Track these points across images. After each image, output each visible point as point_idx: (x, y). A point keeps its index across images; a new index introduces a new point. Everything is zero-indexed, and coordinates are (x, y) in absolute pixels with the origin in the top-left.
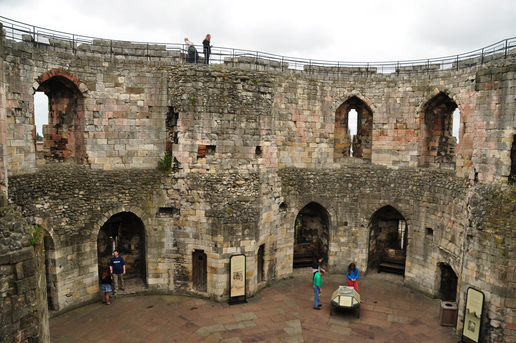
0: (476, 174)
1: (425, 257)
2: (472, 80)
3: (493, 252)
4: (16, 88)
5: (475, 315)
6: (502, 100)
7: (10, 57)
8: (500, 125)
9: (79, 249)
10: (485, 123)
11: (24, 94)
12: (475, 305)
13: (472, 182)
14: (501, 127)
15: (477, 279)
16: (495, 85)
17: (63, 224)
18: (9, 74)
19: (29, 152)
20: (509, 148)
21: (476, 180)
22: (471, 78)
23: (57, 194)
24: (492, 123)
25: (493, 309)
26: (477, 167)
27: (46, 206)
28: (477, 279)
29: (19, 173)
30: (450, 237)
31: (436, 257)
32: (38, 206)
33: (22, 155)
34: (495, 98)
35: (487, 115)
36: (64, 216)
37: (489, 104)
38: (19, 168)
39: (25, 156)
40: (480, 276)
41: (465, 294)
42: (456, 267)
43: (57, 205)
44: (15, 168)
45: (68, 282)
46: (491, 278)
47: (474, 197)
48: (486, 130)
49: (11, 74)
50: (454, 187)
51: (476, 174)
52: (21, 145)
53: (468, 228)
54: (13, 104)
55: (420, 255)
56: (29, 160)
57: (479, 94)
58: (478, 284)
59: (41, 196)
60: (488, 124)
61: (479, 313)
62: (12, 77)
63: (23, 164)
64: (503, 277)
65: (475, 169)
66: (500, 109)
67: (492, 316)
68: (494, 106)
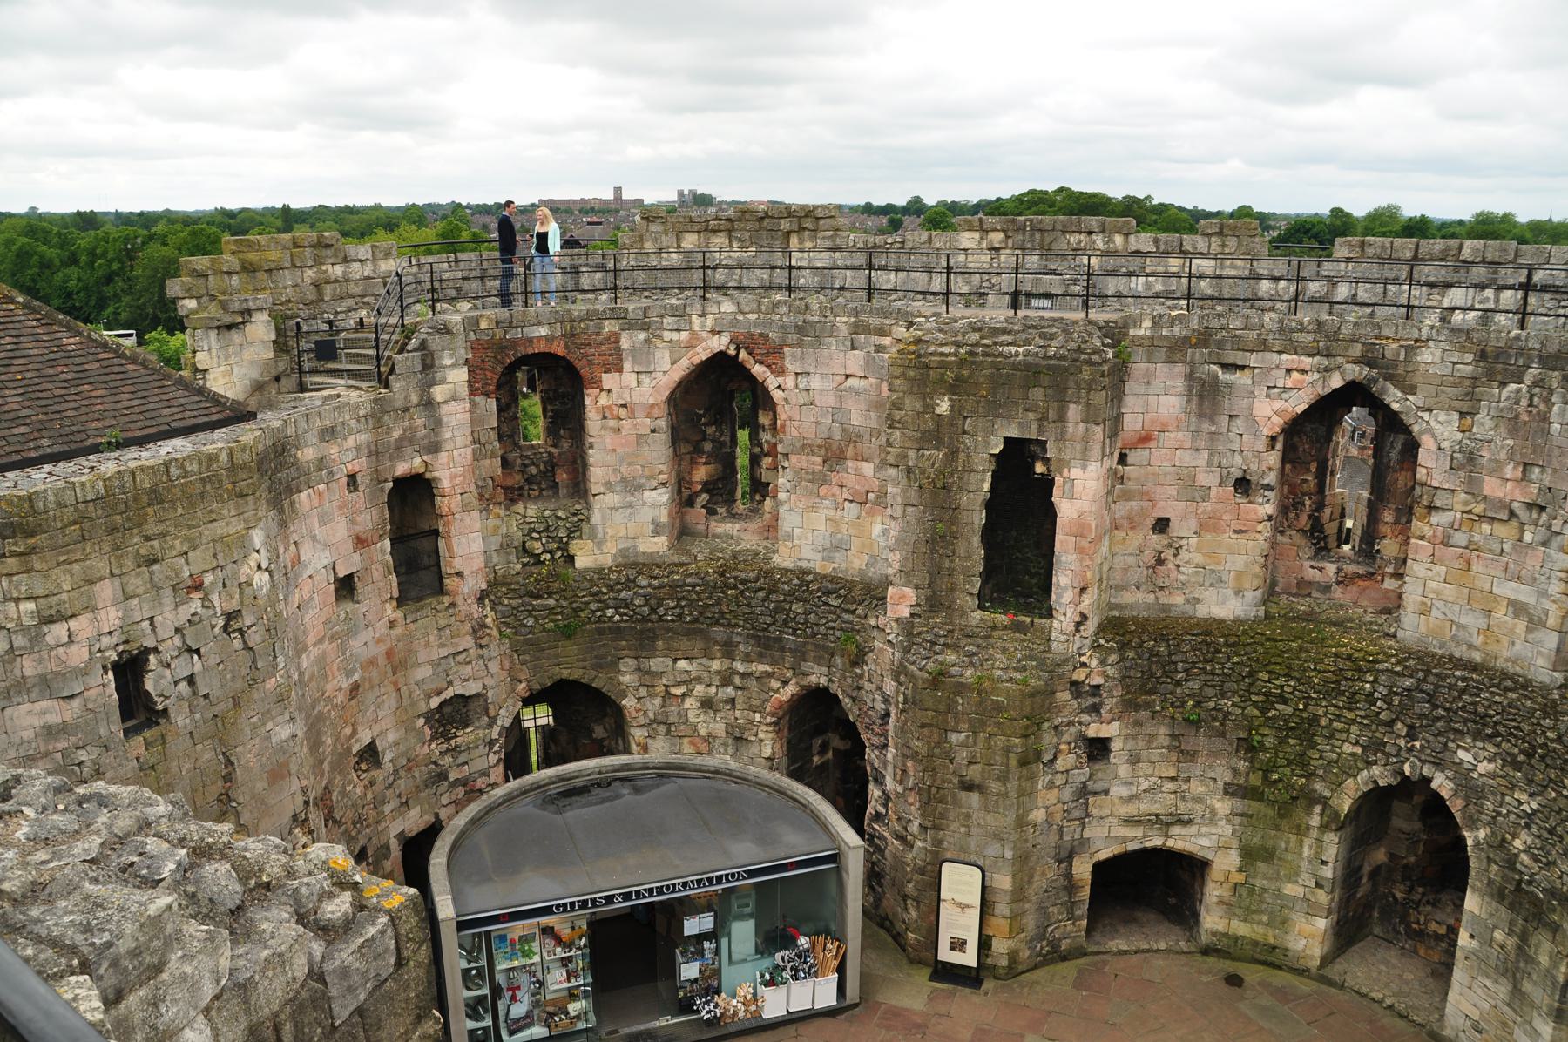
4: (1534, 452)
7: (1533, 372)
9: (1524, 937)
11: (1555, 471)
17: (1517, 843)
18: (1517, 417)
19: (1543, 624)
23: (1521, 758)
27: (1484, 767)
29: (1500, 663)
32: (1462, 754)
33: (1521, 626)
36: (1528, 826)
38: (1506, 654)
39: (1529, 630)
43: (1512, 787)
44: (1493, 648)
45: (1479, 991)
49: (1524, 417)
52: (1523, 598)
54: (1517, 492)
56: (1539, 644)
59: (1477, 736)
62: (1525, 423)
63: (1518, 647)
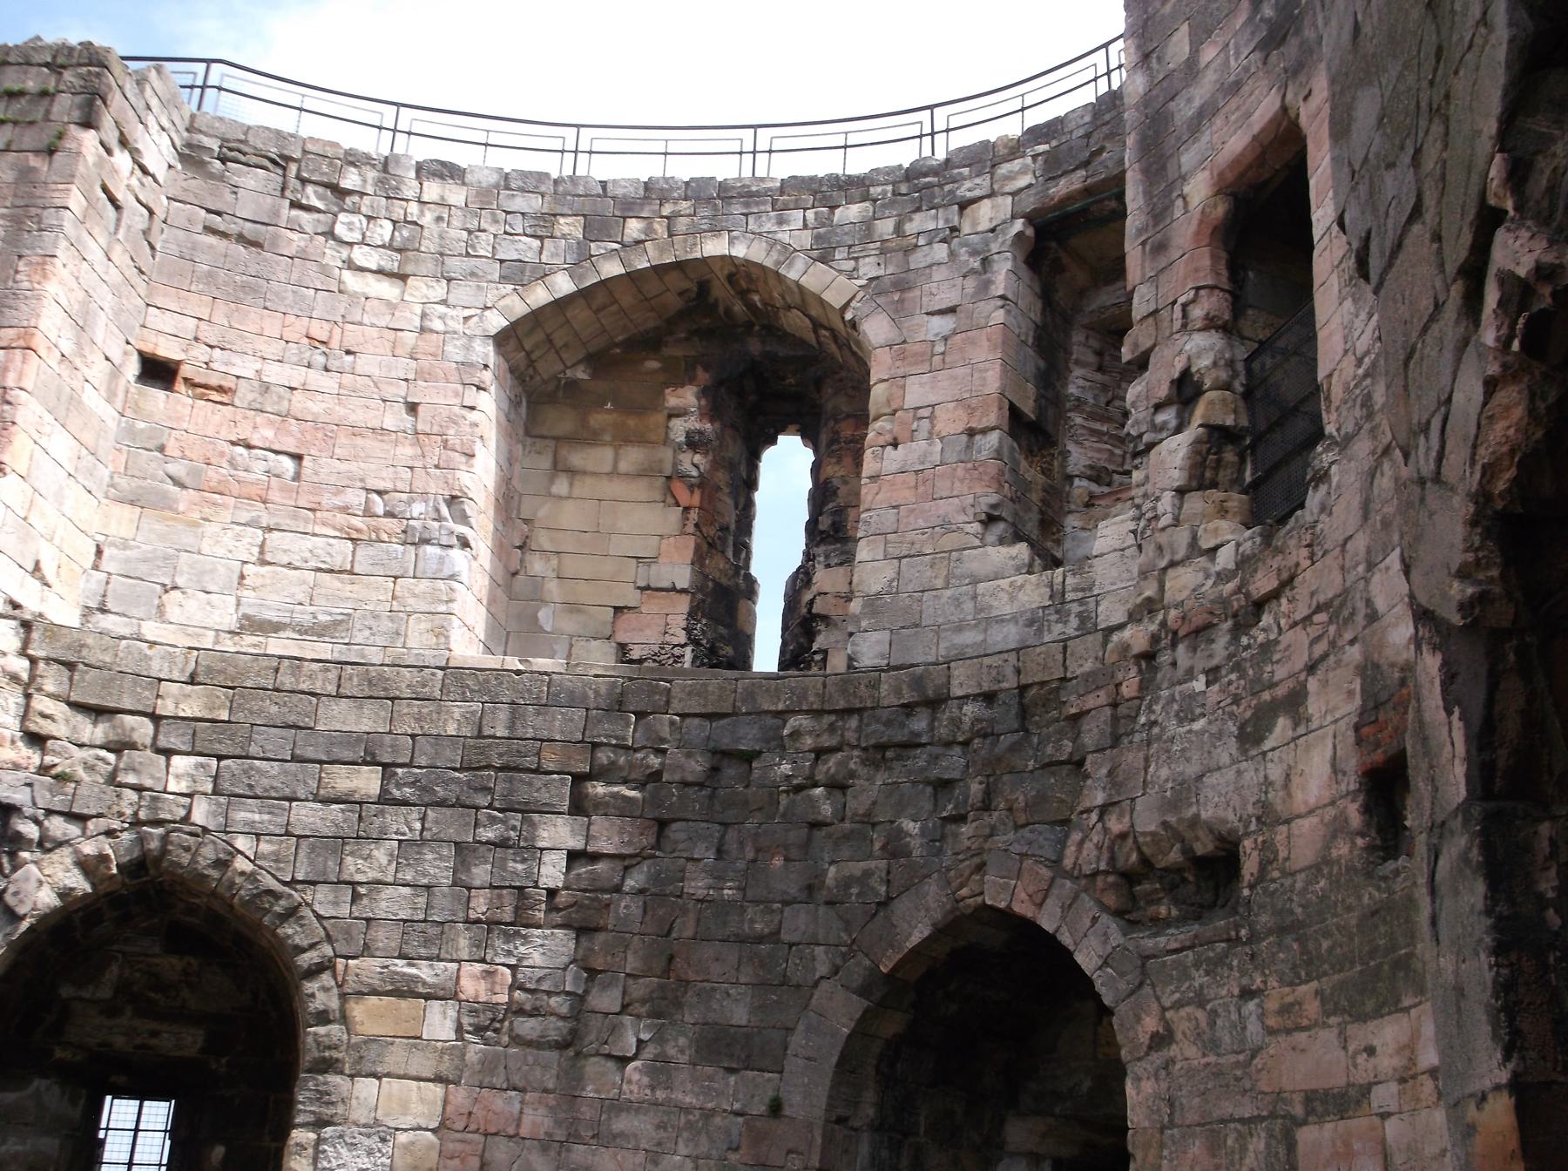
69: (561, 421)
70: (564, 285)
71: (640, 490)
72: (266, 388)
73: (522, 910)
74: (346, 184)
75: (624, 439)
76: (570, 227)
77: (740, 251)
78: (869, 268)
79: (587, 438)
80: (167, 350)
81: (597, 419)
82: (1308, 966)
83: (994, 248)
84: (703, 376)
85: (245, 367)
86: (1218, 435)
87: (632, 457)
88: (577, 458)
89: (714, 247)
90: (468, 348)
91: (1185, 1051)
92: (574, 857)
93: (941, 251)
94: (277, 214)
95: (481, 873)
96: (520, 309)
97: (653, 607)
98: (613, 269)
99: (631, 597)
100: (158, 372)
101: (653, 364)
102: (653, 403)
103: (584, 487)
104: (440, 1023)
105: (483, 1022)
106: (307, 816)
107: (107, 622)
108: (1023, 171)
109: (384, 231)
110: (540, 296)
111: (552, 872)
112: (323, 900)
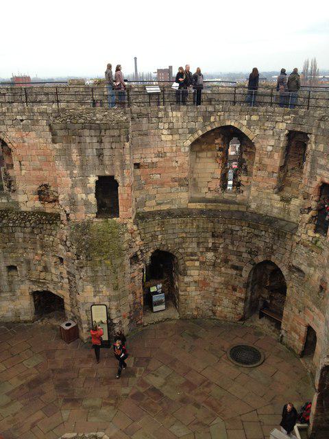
0: (68, 215)
1: (12, 291)
2: (22, 120)
3: (105, 272)
5: (102, 323)
6: (81, 152)
8: (83, 174)
10: (68, 172)
12: (99, 315)
13: (65, 222)
14: (85, 177)
15: (95, 296)
16: (73, 139)
20: (94, 191)
21: (68, 220)
22: (19, 117)
24: (75, 172)
25: (113, 312)
26: (68, 210)
28: (95, 296)
30: (40, 268)
31: (26, 288)
34: (75, 151)
35: (69, 164)
37: (70, 155)
40: (96, 293)
41: (86, 311)
42: (59, 291)
46: (106, 291)
47: (72, 234)
48: (71, 177)
50: (31, 224)
51: (68, 215)
53: (76, 261)
55: (7, 292)
57: (57, 146)
58: (96, 300)
60: (71, 173)
61: (104, 320)
64: (116, 288)
65: (65, 211)
66: (82, 161)
67: (113, 316)
68: (75, 156)
69: (197, 148)
70: (200, 133)
71: (211, 160)
72: (153, 163)
73: (208, 250)
74: (159, 116)
75: (209, 150)
76: (200, 119)
77: (232, 124)
78: (257, 132)
79: (202, 151)
80: (138, 162)
81: (203, 147)
82: (310, 294)
83: (282, 135)
84: (222, 136)
85: (149, 161)
86: (313, 217)
87: (209, 154)
88: (200, 155)
89: (228, 123)
90: (185, 149)
91: (294, 290)
92: (213, 243)
93: (271, 132)
94: (149, 127)
95: (201, 245)
96: (193, 140)
97: (214, 181)
98: (209, 129)
99: (210, 179)
100: (137, 166)
101: (213, 134)
102: (213, 142)
103: (202, 160)
104: (197, 264)
105: (202, 263)
106: (177, 240)
107: (139, 210)
108: (289, 119)
109: (166, 126)
110: (196, 136)
111: (210, 245)
112: (180, 251)
